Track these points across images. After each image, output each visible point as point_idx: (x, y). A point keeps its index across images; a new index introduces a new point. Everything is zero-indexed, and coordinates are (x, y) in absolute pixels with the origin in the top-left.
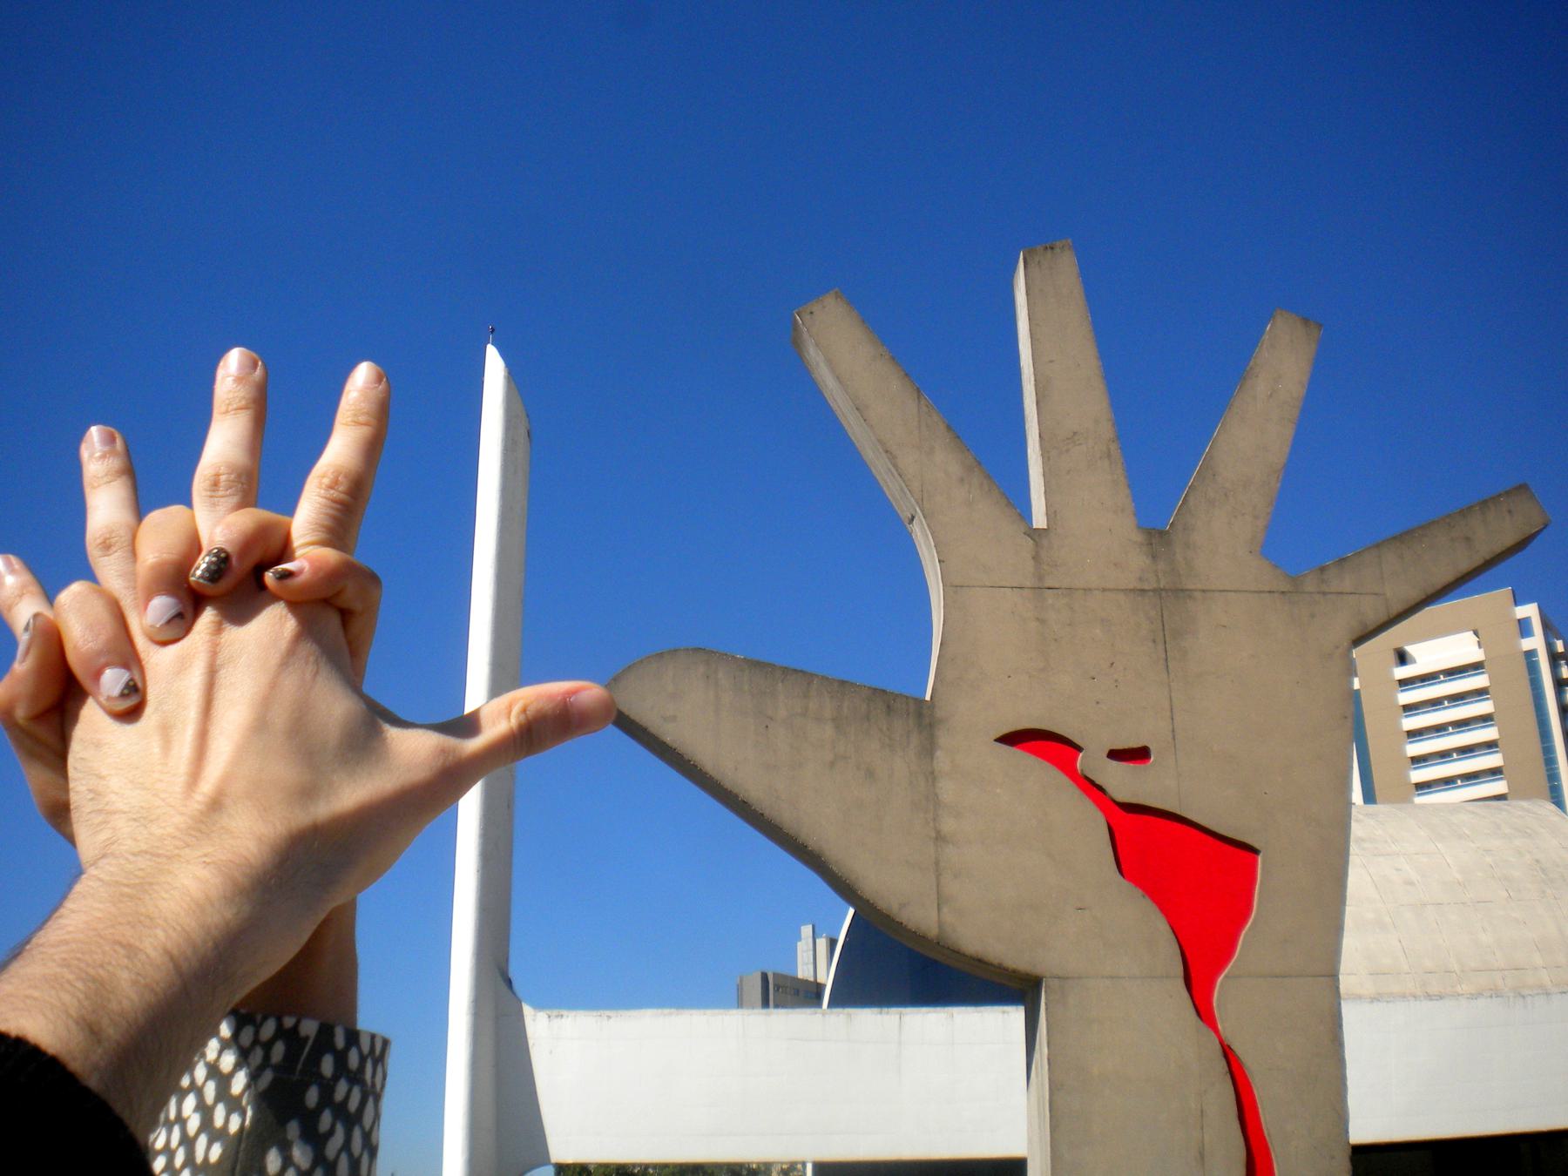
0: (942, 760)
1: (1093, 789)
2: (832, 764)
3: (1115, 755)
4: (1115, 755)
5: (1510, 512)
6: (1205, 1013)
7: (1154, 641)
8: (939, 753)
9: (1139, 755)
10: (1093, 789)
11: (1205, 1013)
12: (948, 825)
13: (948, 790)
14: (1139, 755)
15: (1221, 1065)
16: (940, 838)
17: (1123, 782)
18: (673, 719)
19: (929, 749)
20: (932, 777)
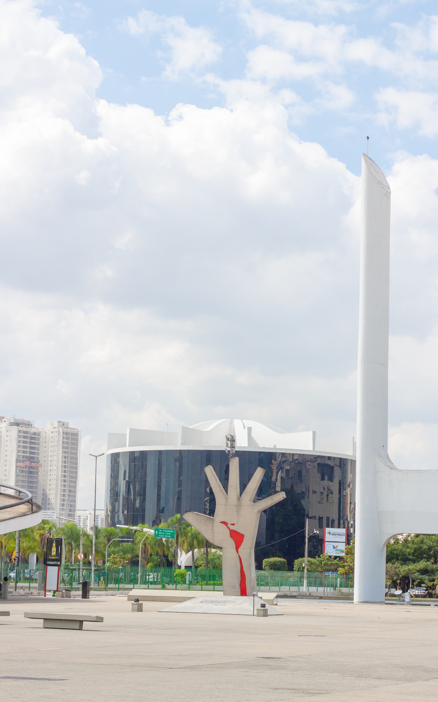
0: (214, 525)
1: (229, 528)
2: (204, 525)
3: (231, 524)
4: (231, 524)
5: (279, 496)
6: (237, 551)
7: (237, 512)
8: (214, 524)
9: (233, 524)
10: (229, 528)
11: (237, 551)
12: (214, 531)
13: (215, 528)
14: (233, 524)
15: (238, 557)
16: (213, 533)
17: (232, 528)
18: (189, 520)
19: (213, 523)
20: (213, 526)
